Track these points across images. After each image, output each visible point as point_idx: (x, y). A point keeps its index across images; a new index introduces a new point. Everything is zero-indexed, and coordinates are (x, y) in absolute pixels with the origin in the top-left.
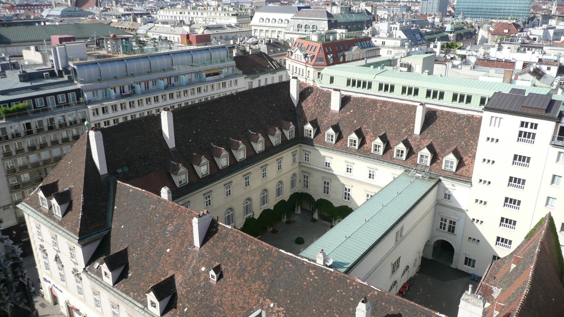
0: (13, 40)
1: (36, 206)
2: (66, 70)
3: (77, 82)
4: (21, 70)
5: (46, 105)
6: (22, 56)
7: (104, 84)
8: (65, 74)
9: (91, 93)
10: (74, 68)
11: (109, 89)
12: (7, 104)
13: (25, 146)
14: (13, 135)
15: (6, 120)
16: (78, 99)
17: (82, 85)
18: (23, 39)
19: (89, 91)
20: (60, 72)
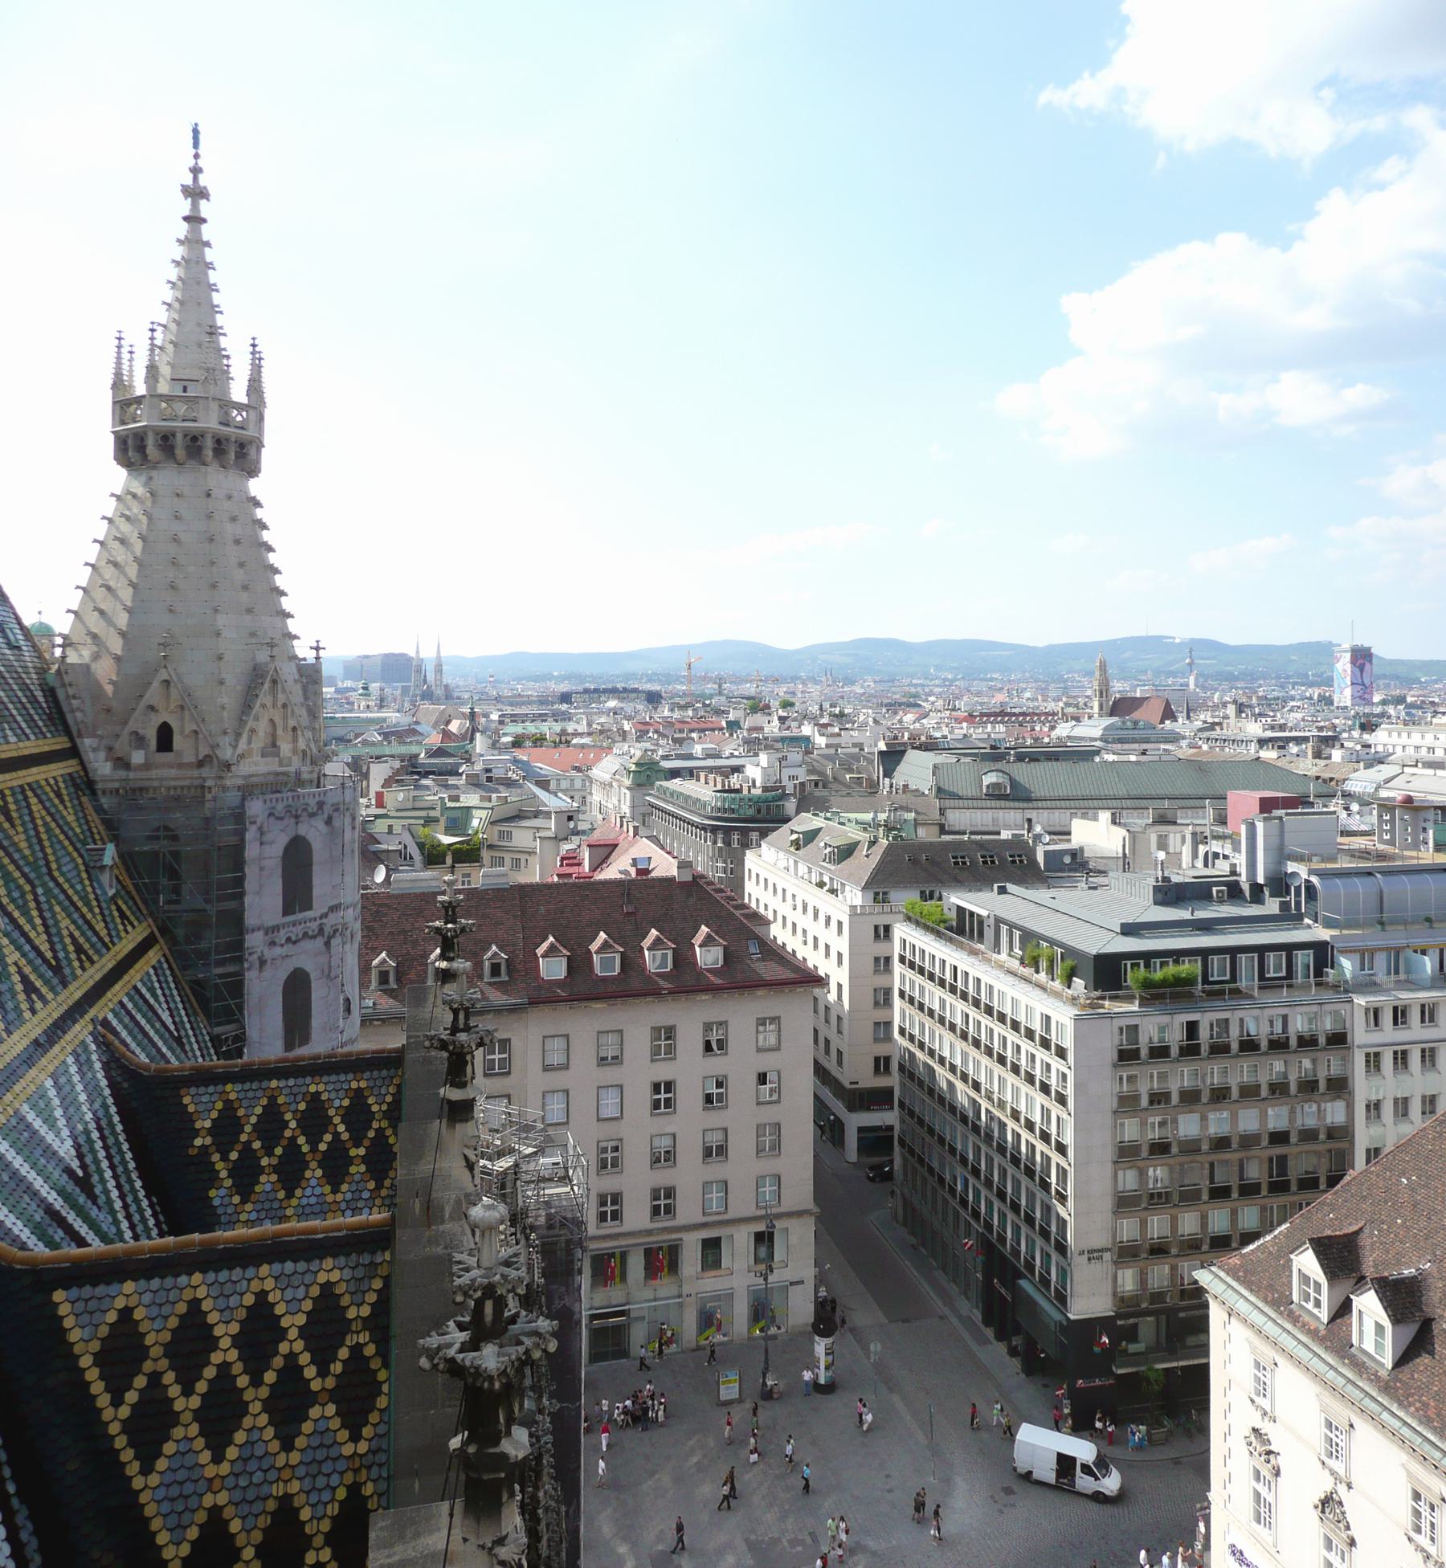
0: (1038, 792)
1: (1279, 1300)
2: (1280, 884)
3: (1310, 922)
4: (1160, 874)
5: (1234, 978)
6: (1069, 833)
7: (1396, 937)
8: (1271, 896)
9: (1357, 957)
10: (1307, 881)
11: (1410, 952)
12: (1142, 962)
13: (1174, 1087)
14: (1151, 1049)
15: (1140, 1006)
16: (1319, 973)
17: (1335, 932)
18: (1062, 793)
19: (1351, 951)
20: (1257, 889)
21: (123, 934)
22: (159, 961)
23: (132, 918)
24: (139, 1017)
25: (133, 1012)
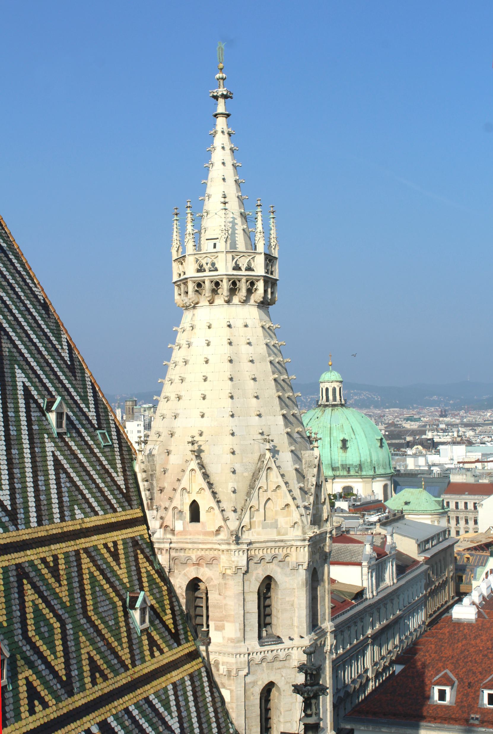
21: (148, 658)
22: (183, 680)
23: (163, 646)
24: (142, 721)
25: (137, 718)
